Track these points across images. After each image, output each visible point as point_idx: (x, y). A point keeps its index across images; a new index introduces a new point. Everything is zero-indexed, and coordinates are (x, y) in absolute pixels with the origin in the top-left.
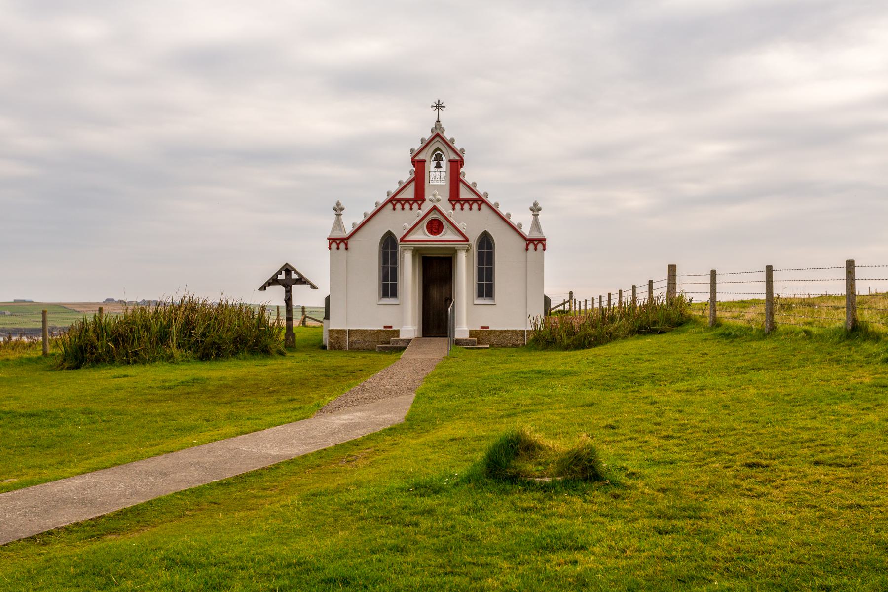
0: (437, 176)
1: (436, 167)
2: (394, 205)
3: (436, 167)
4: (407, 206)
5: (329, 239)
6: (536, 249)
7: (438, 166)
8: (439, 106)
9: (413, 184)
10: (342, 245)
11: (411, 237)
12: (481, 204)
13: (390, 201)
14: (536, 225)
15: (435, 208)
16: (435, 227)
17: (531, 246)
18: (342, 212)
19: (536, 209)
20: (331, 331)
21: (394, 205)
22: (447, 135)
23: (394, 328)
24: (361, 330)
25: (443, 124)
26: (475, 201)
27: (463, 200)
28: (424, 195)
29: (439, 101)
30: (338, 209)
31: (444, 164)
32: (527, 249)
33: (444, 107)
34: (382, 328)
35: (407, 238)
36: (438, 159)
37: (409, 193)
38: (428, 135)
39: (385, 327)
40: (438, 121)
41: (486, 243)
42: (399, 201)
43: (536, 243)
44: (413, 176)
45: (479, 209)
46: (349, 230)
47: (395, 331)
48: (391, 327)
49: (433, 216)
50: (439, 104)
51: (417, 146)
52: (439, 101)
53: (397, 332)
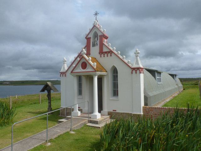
6: (136, 73)
8: (96, 14)
10: (64, 75)
11: (76, 71)
17: (134, 72)
26: (109, 52)
27: (104, 52)
32: (132, 73)
35: (74, 72)
38: (91, 27)
41: (115, 71)
43: (136, 70)
45: (111, 56)
49: (83, 61)
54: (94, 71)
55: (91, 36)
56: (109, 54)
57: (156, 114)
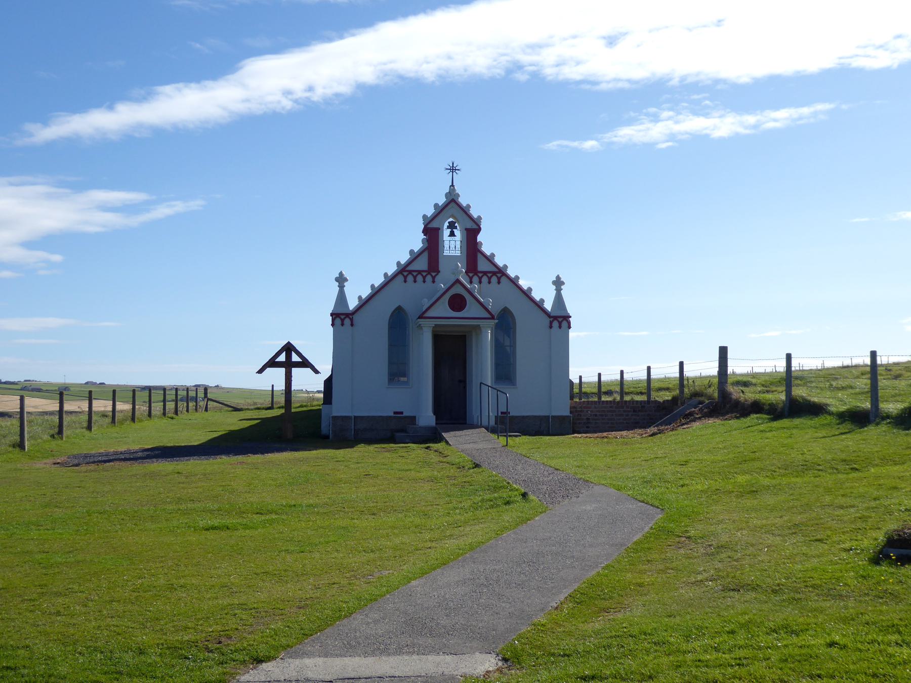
0: (452, 246)
1: (449, 236)
2: (405, 277)
3: (449, 236)
4: (420, 278)
5: (332, 315)
6: (560, 327)
7: (452, 234)
8: (453, 169)
9: (426, 254)
10: (347, 321)
12: (501, 276)
14: (559, 300)
15: (458, 281)
16: (457, 303)
17: (555, 324)
18: (345, 284)
19: (558, 283)
20: (335, 418)
21: (405, 277)
22: (463, 201)
23: (405, 414)
24: (368, 417)
25: (458, 189)
26: (494, 273)
29: (453, 164)
30: (341, 280)
31: (457, 232)
32: (551, 327)
33: (458, 170)
34: (392, 414)
36: (452, 226)
37: (422, 264)
38: (442, 201)
39: (395, 413)
40: (452, 185)
42: (410, 272)
43: (560, 320)
44: (426, 245)
45: (499, 283)
46: (352, 304)
47: (406, 417)
48: (402, 413)
49: (458, 290)
50: (453, 167)
51: (430, 212)
52: (453, 164)
53: (413, 419)
54: (490, 316)
56: (494, 279)
57: (596, 415)
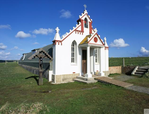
4: (79, 33)
10: (60, 43)
13: (75, 30)
21: (76, 32)
23: (76, 73)
28: (83, 31)
32: (105, 49)
37: (80, 29)
39: (73, 73)
42: (77, 31)
48: (75, 73)
55: (83, 19)
